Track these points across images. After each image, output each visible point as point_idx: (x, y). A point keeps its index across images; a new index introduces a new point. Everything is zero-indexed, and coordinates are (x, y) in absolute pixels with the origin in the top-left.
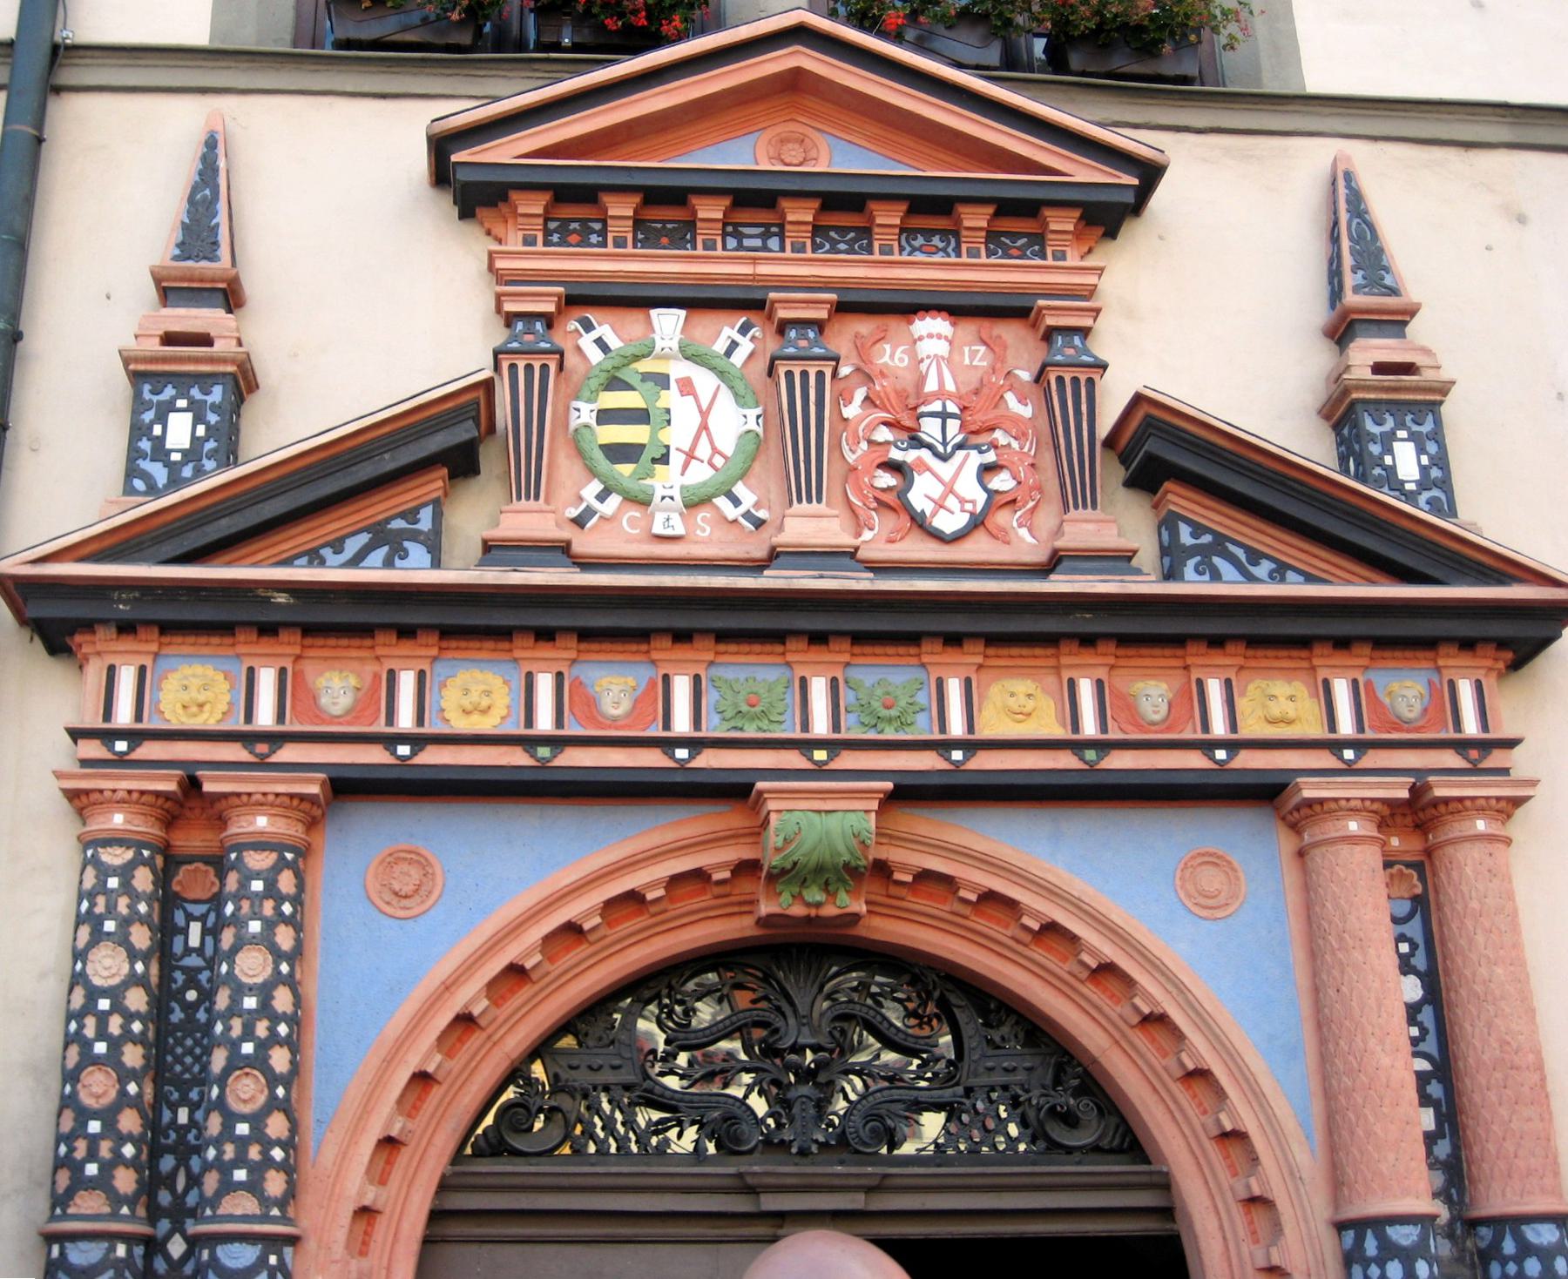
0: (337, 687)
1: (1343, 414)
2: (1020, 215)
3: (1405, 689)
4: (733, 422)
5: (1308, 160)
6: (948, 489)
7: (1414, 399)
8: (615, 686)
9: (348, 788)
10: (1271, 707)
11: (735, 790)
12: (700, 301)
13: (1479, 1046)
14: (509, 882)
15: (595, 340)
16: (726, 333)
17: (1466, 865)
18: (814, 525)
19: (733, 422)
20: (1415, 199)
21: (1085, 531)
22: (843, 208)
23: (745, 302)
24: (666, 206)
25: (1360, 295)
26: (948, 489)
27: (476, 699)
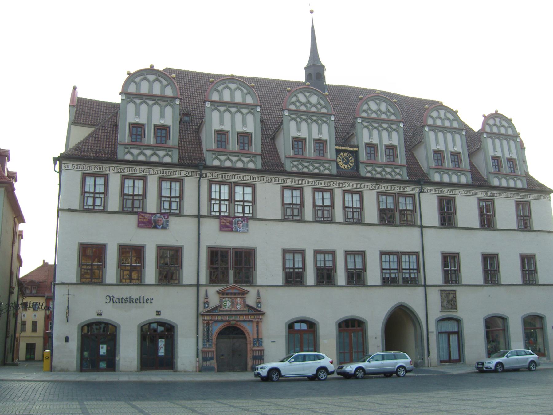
0: (214, 317)
2: (243, 294)
3: (258, 317)
4: (230, 304)
5: (257, 288)
6: (239, 307)
8: (225, 317)
9: (215, 321)
10: (252, 317)
12: (228, 298)
13: (259, 331)
15: (224, 300)
17: (260, 324)
18: (233, 309)
19: (230, 304)
20: (262, 291)
21: (245, 309)
22: (235, 294)
23: (231, 298)
24: (227, 294)
25: (258, 296)
27: (219, 318)
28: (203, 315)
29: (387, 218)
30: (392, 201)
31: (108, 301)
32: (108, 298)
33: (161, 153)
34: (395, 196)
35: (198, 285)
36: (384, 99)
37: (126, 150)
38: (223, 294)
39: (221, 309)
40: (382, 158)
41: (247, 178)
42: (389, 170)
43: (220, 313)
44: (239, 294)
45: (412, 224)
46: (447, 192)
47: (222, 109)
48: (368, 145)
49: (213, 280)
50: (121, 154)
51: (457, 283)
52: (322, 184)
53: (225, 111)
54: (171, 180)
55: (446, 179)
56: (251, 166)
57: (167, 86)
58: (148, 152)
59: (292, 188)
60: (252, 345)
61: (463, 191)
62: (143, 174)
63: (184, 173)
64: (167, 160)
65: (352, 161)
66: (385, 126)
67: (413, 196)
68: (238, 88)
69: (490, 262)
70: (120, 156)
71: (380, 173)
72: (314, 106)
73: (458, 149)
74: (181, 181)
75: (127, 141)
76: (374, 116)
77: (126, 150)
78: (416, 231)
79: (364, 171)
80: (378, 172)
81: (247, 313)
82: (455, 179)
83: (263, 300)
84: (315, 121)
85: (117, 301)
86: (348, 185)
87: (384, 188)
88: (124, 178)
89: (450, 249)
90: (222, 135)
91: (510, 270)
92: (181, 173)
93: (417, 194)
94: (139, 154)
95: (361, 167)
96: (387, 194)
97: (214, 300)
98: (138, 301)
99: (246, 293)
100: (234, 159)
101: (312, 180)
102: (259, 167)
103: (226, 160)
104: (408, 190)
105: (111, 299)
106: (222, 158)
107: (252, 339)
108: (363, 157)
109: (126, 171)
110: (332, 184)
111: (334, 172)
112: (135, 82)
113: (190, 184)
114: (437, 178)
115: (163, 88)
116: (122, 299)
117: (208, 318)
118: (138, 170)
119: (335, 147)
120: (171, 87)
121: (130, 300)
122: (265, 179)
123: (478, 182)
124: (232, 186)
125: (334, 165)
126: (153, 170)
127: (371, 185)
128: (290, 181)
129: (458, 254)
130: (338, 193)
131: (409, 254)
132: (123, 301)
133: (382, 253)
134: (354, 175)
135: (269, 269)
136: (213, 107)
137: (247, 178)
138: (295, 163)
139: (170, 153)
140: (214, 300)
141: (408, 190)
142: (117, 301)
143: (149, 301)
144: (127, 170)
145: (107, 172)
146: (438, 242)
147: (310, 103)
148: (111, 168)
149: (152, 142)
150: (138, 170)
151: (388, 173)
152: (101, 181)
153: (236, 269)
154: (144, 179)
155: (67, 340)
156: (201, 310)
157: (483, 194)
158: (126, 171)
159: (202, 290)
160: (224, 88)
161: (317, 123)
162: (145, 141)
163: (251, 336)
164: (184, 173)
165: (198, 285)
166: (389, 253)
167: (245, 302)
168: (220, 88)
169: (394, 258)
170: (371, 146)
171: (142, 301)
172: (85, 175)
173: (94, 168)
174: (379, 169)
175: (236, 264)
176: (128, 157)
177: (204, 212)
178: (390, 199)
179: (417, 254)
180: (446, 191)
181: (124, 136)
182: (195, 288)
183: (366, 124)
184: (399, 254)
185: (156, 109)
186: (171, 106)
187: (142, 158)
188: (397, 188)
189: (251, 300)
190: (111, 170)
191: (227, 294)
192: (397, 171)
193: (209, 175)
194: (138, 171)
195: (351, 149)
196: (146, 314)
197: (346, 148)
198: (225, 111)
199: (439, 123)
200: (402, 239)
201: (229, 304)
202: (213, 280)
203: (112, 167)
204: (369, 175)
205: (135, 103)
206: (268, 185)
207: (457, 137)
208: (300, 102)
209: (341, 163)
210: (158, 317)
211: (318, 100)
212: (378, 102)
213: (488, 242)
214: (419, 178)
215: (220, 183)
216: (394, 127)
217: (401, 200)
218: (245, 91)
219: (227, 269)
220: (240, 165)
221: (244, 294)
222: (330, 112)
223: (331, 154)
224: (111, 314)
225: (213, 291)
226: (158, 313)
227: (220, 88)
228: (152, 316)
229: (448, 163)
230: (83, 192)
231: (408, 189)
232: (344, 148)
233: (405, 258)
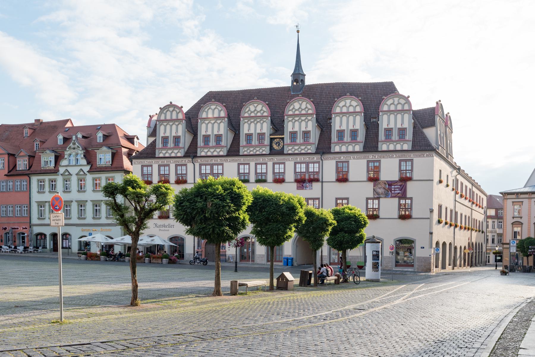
42: (303, 147)
46: (343, 158)
48: (291, 133)
52: (261, 160)
54: (181, 165)
55: (344, 149)
56: (221, 153)
59: (244, 164)
61: (355, 156)
74: (186, 165)
78: (320, 184)
79: (288, 149)
80: (296, 149)
82: (350, 149)
86: (276, 159)
87: (299, 159)
92: (185, 161)
101: (254, 158)
104: (315, 159)
108: (287, 140)
110: (266, 159)
113: (190, 166)
124: (212, 166)
125: (268, 148)
126: (172, 160)
127: (290, 157)
128: (242, 160)
130: (270, 164)
134: (281, 153)
137: (219, 160)
138: (246, 149)
141: (315, 159)
144: (160, 161)
151: (303, 149)
154: (169, 165)
157: (371, 156)
162: (169, 146)
170: (293, 135)
173: (146, 162)
174: (296, 147)
176: (161, 155)
180: (342, 158)
188: (307, 158)
193: (199, 161)
194: (165, 161)
195: (280, 136)
197: (277, 137)
203: (153, 161)
204: (290, 152)
209: (275, 146)
215: (206, 165)
217: (311, 165)
220: (215, 154)
223: (267, 142)
231: (316, 158)
232: (275, 137)
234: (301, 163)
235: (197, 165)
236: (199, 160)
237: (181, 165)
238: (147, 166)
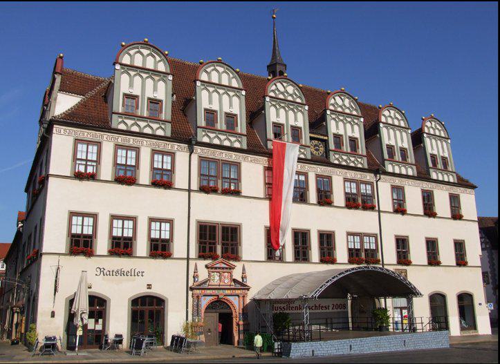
0: (203, 291)
1: (242, 278)
5: (243, 263)
6: (226, 281)
7: (245, 277)
10: (238, 292)
11: (218, 296)
14: (209, 299)
16: (219, 274)
18: (221, 284)
19: (218, 278)
20: (247, 266)
22: (223, 268)
26: (226, 281)
27: (208, 292)
28: (192, 289)
29: (352, 202)
30: (355, 186)
31: (98, 273)
32: (98, 270)
33: (155, 126)
34: (358, 183)
35: (188, 259)
36: (347, 96)
37: (120, 120)
38: (212, 268)
39: (210, 284)
40: (346, 147)
41: (234, 156)
42: (353, 159)
43: (209, 287)
44: (227, 268)
45: (372, 208)
46: (397, 181)
47: (211, 89)
49: (202, 256)
50: (117, 123)
51: (408, 263)
53: (213, 91)
56: (237, 145)
57: (160, 61)
58: (142, 124)
60: (238, 319)
61: (411, 181)
62: (136, 145)
63: (176, 147)
64: (160, 133)
65: (322, 149)
66: (349, 120)
67: (371, 184)
68: (224, 72)
69: (432, 245)
70: (114, 125)
71: (346, 161)
72: (291, 95)
73: (406, 145)
74: (172, 155)
75: (120, 111)
76: (339, 109)
77: (120, 120)
78: (374, 215)
79: (334, 158)
81: (234, 287)
83: (247, 274)
84: (292, 110)
85: (108, 273)
86: (321, 170)
87: (351, 174)
88: (118, 147)
89: (402, 233)
90: (211, 114)
91: (447, 254)
93: (375, 182)
94: (133, 125)
95: (331, 153)
96: (351, 181)
97: (203, 274)
98: (129, 274)
99: (233, 268)
100: (223, 137)
102: (245, 147)
103: (215, 137)
105: (102, 270)
106: (212, 135)
107: (238, 314)
109: (119, 140)
111: (309, 157)
112: (129, 55)
114: (389, 168)
115: (156, 63)
116: (113, 271)
117: (198, 292)
118: (132, 140)
119: (308, 135)
120: (164, 63)
121: (121, 273)
122: (250, 159)
123: (423, 176)
126: (145, 141)
129: (408, 237)
131: (369, 235)
132: (114, 273)
133: (349, 234)
135: (252, 244)
136: (203, 87)
137: (234, 157)
139: (163, 126)
140: (203, 274)
142: (108, 273)
143: (140, 274)
144: (121, 139)
145: (100, 140)
146: (394, 226)
147: (288, 93)
148: (105, 136)
149: (145, 114)
150: (132, 140)
152: (93, 149)
153: (223, 244)
154: (137, 150)
155: (53, 315)
156: (191, 284)
157: (427, 186)
158: (119, 140)
159: (192, 263)
160: (213, 70)
161: (293, 111)
163: (237, 310)
164: (176, 147)
165: (188, 259)
166: (354, 234)
167: (231, 276)
168: (209, 70)
169: (357, 239)
170: (338, 137)
171: (133, 274)
172: (77, 141)
174: (345, 157)
175: (223, 239)
176: (122, 127)
177: (195, 186)
178: (354, 185)
179: (375, 236)
180: (397, 181)
181: (119, 105)
182: (186, 261)
183: (334, 116)
184: (361, 235)
185: (149, 82)
186: (164, 81)
187: (135, 129)
188: (358, 175)
189: (237, 275)
190: (105, 139)
191: (216, 268)
192: (359, 160)
193: (199, 151)
194: (131, 141)
195: (322, 137)
196: (138, 288)
198: (213, 91)
199: (390, 121)
200: (363, 221)
201: (217, 278)
202: (202, 256)
203: (106, 135)
204: (336, 162)
205: (129, 74)
206: (252, 165)
207: (404, 134)
208: (279, 91)
210: (149, 290)
211: (294, 91)
212: (343, 97)
213: (430, 228)
214: (377, 169)
216: (356, 121)
218: (231, 75)
219: (214, 244)
220: (227, 143)
221: (232, 268)
222: (304, 102)
224: (101, 287)
225: (202, 263)
226: (149, 286)
227: (209, 70)
228: (141, 290)
229: (398, 157)
230: (75, 159)
231: (369, 177)
232: (315, 136)
233: (366, 239)
234: (351, 181)
235: (195, 158)
236: (198, 149)
237: (163, 153)
238: (88, 143)
